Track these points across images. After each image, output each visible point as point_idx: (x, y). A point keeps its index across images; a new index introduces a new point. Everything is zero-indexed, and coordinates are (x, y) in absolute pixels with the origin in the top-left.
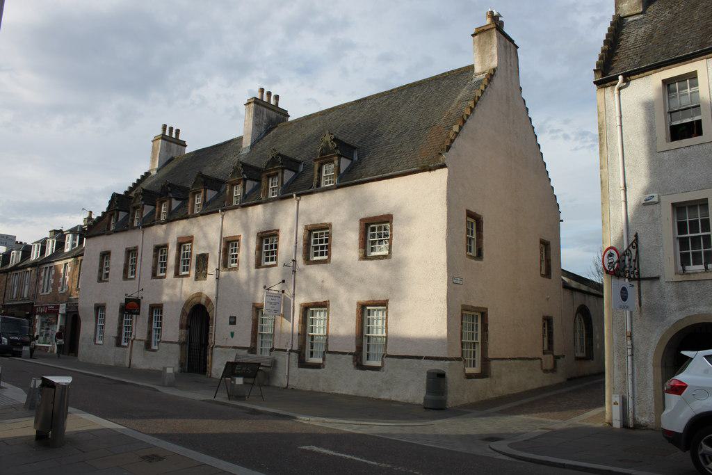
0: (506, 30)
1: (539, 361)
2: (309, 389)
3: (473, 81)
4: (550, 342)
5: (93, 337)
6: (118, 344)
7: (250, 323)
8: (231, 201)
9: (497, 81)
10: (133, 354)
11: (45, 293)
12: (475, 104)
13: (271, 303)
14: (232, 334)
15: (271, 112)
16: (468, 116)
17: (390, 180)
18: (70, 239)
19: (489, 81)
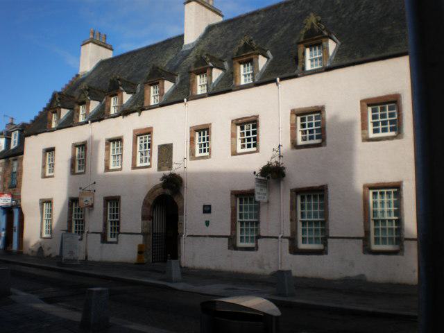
7: (229, 211)
14: (207, 223)
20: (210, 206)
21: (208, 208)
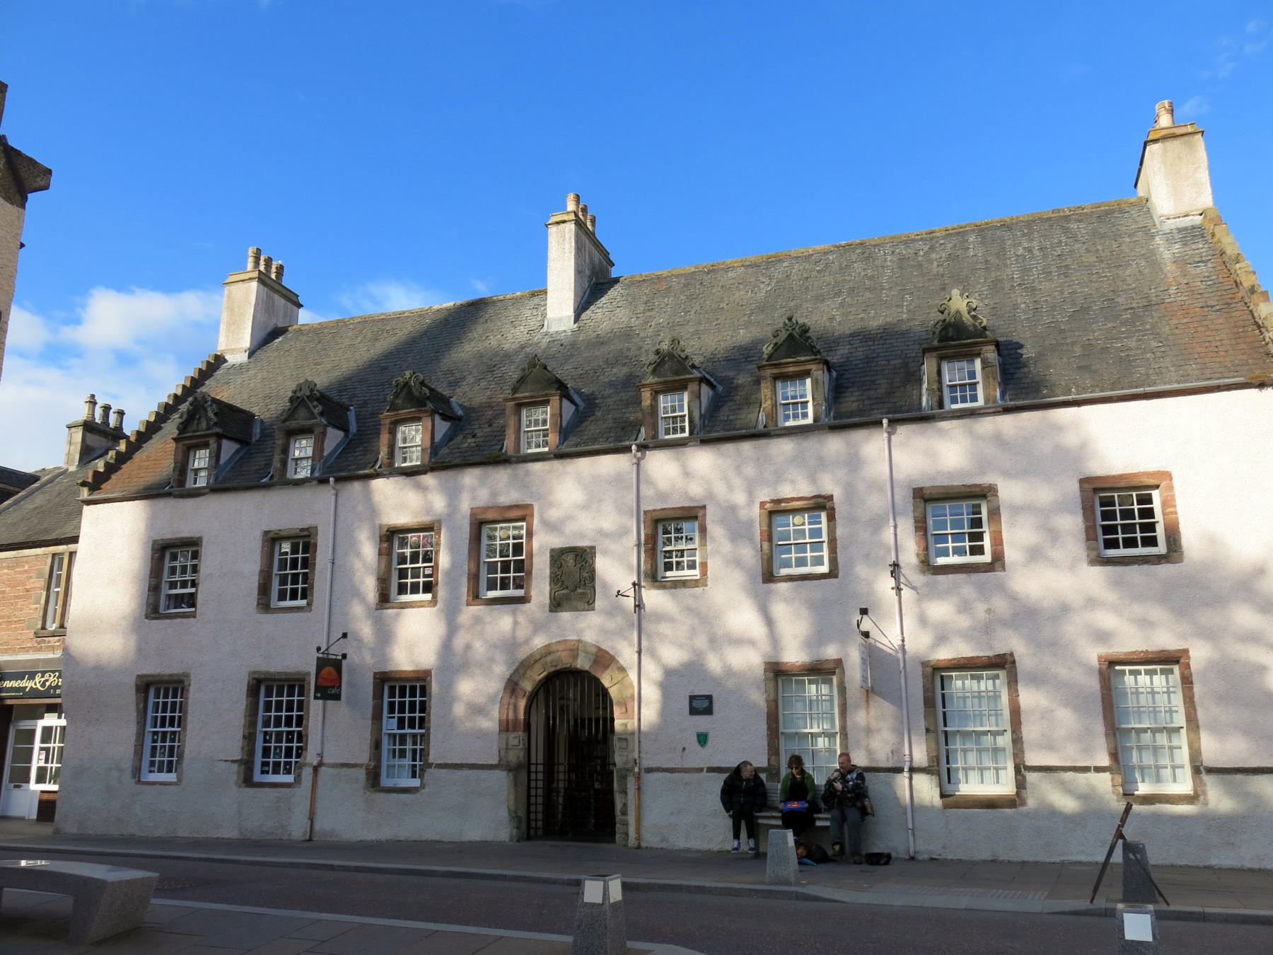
2: (984, 855)
5: (128, 764)
14: (703, 739)
21: (706, 704)
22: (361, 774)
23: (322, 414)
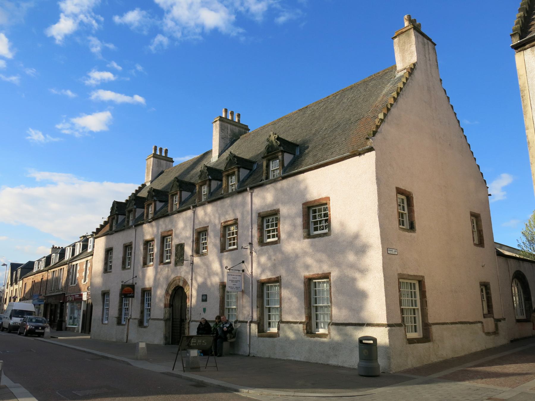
0: (422, 30)
1: (479, 325)
2: (267, 356)
3: (396, 78)
4: (490, 306)
5: (101, 318)
6: (119, 323)
8: (200, 199)
9: (416, 73)
10: (130, 331)
11: (73, 285)
12: (398, 94)
13: (232, 281)
14: (204, 310)
15: (234, 127)
16: (392, 105)
17: (326, 167)
18: (92, 241)
19: (410, 74)
20: (206, 295)
22: (137, 321)
23: (135, 204)
